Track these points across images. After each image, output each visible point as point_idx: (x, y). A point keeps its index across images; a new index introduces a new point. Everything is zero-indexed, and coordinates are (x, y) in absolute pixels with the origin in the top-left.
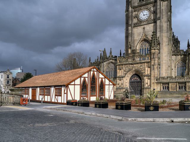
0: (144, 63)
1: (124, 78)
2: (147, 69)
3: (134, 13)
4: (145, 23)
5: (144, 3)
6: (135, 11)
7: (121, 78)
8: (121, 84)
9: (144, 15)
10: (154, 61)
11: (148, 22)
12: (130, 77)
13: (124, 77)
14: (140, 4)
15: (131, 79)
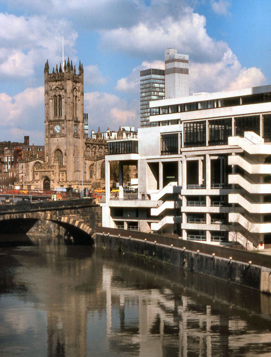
0: (51, 171)
1: (39, 181)
2: (52, 175)
3: (51, 125)
4: (57, 136)
5: (57, 119)
6: (51, 124)
7: (37, 181)
8: (38, 185)
9: (57, 128)
10: (56, 170)
11: (62, 135)
12: (43, 180)
13: (39, 180)
14: (55, 119)
15: (44, 182)
